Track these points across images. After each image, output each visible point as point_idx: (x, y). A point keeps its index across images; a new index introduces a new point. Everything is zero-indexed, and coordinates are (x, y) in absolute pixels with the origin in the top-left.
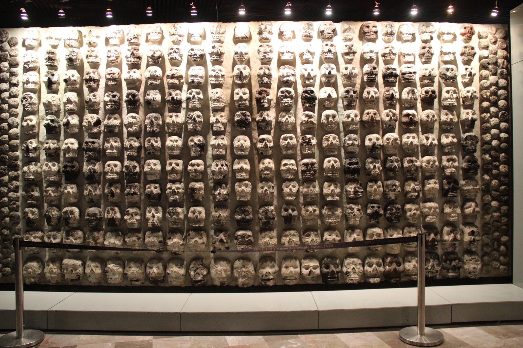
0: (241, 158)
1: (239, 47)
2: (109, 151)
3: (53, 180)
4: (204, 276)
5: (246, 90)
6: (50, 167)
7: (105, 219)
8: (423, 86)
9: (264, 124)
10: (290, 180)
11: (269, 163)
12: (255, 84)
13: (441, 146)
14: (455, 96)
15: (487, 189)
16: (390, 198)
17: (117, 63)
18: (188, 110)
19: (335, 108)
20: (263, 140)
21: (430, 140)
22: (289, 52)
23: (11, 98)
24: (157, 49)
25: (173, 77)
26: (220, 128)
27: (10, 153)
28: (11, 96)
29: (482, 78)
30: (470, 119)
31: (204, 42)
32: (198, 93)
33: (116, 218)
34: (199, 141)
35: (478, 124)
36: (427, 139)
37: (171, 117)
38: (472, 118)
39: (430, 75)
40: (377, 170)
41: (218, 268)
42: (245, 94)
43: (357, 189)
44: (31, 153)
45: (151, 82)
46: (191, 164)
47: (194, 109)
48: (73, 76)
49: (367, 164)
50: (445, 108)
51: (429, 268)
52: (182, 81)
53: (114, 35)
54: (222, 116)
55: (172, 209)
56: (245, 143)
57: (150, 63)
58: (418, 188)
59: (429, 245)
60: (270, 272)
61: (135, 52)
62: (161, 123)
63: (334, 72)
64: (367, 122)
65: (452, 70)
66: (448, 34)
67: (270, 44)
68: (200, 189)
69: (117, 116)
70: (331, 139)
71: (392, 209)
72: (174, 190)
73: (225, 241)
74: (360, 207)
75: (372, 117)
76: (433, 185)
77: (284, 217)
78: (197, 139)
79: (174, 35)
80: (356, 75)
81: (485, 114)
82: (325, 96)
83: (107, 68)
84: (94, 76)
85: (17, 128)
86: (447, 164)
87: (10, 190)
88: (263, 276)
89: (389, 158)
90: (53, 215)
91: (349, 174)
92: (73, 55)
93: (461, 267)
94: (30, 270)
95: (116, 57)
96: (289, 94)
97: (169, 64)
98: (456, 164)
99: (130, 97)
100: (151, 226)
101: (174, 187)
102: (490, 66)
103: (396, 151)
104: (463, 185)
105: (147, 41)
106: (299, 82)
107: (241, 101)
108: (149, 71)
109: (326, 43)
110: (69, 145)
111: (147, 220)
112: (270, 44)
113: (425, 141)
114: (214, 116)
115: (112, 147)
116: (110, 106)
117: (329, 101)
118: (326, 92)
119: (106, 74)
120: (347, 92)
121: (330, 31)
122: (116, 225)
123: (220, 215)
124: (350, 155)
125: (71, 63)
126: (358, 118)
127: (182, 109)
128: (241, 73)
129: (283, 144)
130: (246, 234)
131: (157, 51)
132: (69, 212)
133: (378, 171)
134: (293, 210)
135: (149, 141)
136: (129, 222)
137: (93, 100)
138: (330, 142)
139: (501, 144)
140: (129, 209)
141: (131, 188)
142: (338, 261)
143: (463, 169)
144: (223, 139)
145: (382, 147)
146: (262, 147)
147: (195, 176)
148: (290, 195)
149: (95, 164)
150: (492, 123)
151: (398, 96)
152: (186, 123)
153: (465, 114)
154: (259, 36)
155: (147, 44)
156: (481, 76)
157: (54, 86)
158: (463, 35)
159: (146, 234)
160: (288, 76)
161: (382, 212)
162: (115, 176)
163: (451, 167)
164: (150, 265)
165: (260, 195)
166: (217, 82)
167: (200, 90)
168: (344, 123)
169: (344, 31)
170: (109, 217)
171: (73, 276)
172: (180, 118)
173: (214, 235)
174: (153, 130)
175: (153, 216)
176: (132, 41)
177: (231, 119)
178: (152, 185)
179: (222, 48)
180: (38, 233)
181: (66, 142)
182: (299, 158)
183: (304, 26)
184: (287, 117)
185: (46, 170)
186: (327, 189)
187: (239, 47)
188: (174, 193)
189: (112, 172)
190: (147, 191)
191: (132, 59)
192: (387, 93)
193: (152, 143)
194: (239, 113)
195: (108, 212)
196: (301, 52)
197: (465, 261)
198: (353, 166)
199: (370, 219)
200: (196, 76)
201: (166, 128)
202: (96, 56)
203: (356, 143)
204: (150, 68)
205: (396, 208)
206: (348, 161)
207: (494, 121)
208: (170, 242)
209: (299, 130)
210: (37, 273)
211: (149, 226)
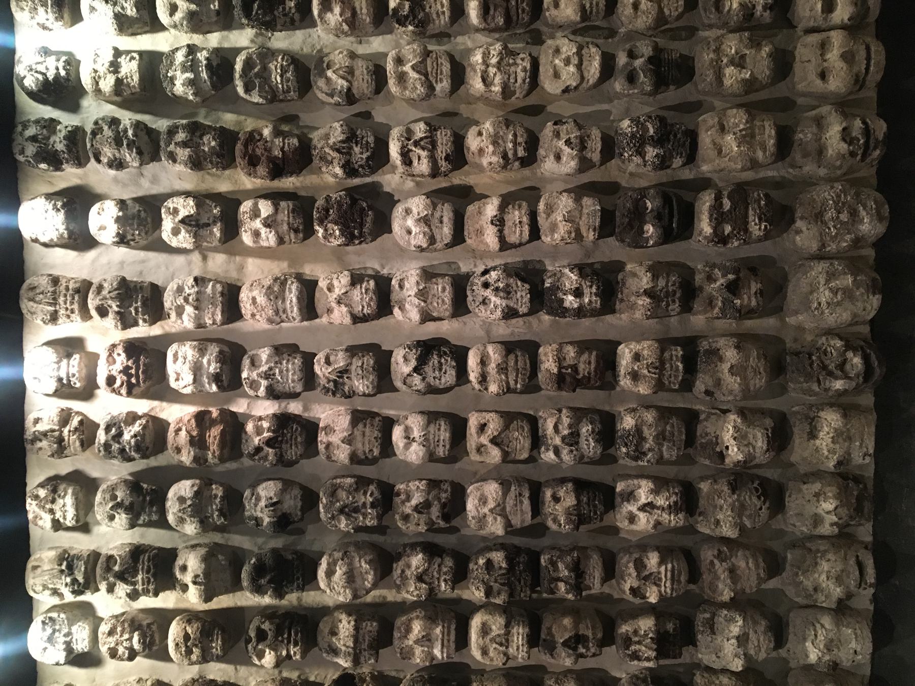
1: (102, 228)
2: (437, 652)
4: (848, 346)
17: (154, 627)
24: (108, 496)
25: (198, 442)
26: (367, 290)
33: (657, 632)
42: (255, 213)
46: (480, 383)
52: (215, 413)
53: (60, 639)
54: (330, 288)
55: (626, 445)
56: (415, 210)
57: (155, 517)
60: (841, 129)
62: (349, 481)
67: (89, 128)
72: (563, 439)
73: (731, 277)
83: (170, 660)
95: (132, 632)
97: (160, 456)
99: (263, 581)
105: (83, 527)
108: (181, 521)
112: (89, 128)
114: (329, 311)
115: (426, 640)
119: (186, 662)
123: (647, 293)
127: (306, 415)
135: (406, 518)
136: (667, 587)
159: (707, 531)
167: (246, 357)
170: (653, 654)
174: (373, 505)
175: (648, 507)
176: (81, 579)
179: (106, 285)
187: (102, 228)
188: (573, 439)
200: (197, 369)
208: (735, 454)
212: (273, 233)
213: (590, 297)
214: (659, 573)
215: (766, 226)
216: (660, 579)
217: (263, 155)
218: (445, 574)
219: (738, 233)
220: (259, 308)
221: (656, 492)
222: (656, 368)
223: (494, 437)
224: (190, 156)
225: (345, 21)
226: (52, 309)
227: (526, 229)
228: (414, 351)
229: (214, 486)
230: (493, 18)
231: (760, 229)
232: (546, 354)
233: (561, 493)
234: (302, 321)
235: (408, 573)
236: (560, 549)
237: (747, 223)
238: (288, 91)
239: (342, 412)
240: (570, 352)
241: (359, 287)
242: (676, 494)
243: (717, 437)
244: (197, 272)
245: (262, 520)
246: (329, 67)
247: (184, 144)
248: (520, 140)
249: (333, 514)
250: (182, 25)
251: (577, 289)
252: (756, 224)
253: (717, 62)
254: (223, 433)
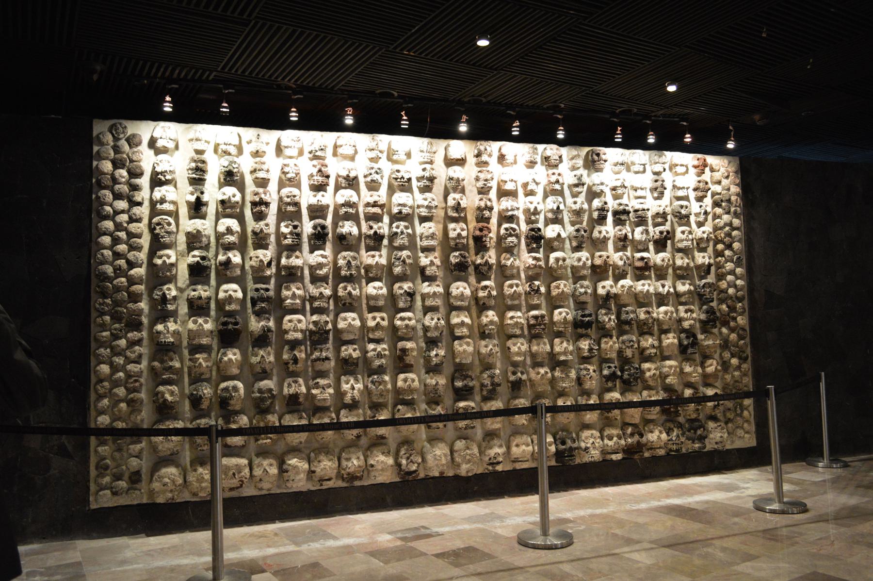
0: (459, 309)
1: (455, 172)
2: (288, 301)
3: (205, 343)
4: (419, 464)
5: (465, 226)
6: (201, 325)
7: (284, 396)
8: (655, 225)
9: (486, 268)
10: (516, 336)
12: (471, 217)
13: (678, 295)
14: (690, 236)
15: (725, 344)
16: (627, 356)
18: (392, 248)
19: (563, 250)
20: (486, 287)
21: (666, 288)
22: (512, 180)
23: (131, 223)
27: (130, 305)
28: (132, 220)
29: (715, 217)
30: (707, 263)
31: (408, 161)
32: (406, 228)
34: (409, 288)
35: (713, 269)
36: (663, 286)
37: (373, 256)
38: (709, 263)
39: (664, 213)
40: (612, 323)
41: (436, 452)
42: (463, 230)
44: (170, 304)
45: (346, 210)
47: (401, 248)
48: (234, 196)
49: (600, 317)
50: (680, 250)
51: (674, 439)
54: (435, 258)
58: (656, 343)
59: (673, 412)
61: (323, 169)
62: (359, 263)
63: (562, 207)
64: (599, 266)
65: (687, 207)
66: (682, 165)
68: (412, 349)
69: (297, 253)
70: (562, 286)
71: (630, 369)
72: (379, 352)
74: (595, 368)
75: (605, 260)
76: (670, 340)
77: (512, 382)
78: (407, 286)
79: (373, 150)
80: (585, 211)
81: (720, 258)
82: (554, 235)
84: (266, 198)
85: (141, 267)
86: (686, 316)
87: (129, 361)
88: (490, 459)
89: (624, 309)
90: (204, 395)
91: (581, 328)
92: (235, 166)
93: (706, 437)
94: (167, 480)
96: (514, 231)
97: (365, 187)
98: (694, 315)
99: (319, 228)
100: (351, 402)
101: (380, 348)
102: (723, 204)
103: (632, 301)
104: (702, 340)
105: (335, 154)
106: (522, 218)
107: (459, 239)
109: (551, 172)
110: (231, 293)
111: (344, 393)
113: (661, 289)
114: (426, 257)
115: (294, 296)
116: (290, 240)
117: (558, 241)
120: (578, 231)
121: (557, 158)
122: (300, 404)
123: (437, 383)
124: (580, 305)
125: (230, 177)
126: (589, 262)
128: (459, 204)
130: (470, 406)
131: (352, 169)
132: (231, 388)
134: (522, 373)
135: (345, 288)
137: (265, 231)
138: (560, 290)
139: (738, 292)
140: (318, 380)
141: (321, 351)
142: (574, 435)
143: (701, 321)
144: (438, 286)
145: (616, 296)
146: (485, 297)
147: (406, 334)
148: (518, 354)
149: (269, 320)
150: (727, 268)
151: (631, 237)
152: (390, 266)
153: (701, 258)
154: (475, 159)
155: (335, 159)
156: (715, 214)
157: (204, 209)
158: (695, 167)
160: (512, 210)
161: (619, 373)
162: (299, 336)
163: (689, 319)
164: (347, 456)
165: (481, 356)
166: (430, 214)
168: (573, 267)
169: (572, 159)
170: (291, 392)
171: (235, 482)
172: (380, 258)
173: (428, 409)
174: (351, 274)
175: (353, 388)
177: (445, 260)
178: (350, 346)
180: (178, 423)
181: (226, 289)
182: (524, 309)
183: (528, 150)
184: (512, 259)
185: (195, 329)
187: (455, 172)
188: (380, 356)
189: (295, 330)
190: (343, 354)
191: (320, 179)
192: (620, 233)
193: (350, 291)
194: (457, 254)
195: (289, 385)
196: (525, 181)
197: (710, 429)
198: (587, 319)
199: (607, 381)
200: (404, 205)
201: (363, 271)
202: (268, 171)
203: (589, 291)
204: (342, 192)
205: (634, 368)
206: (580, 313)
207: (729, 266)
209: (523, 275)
210: (178, 483)
211: (346, 402)
213: (435, 360)
226: (425, 151)
227: (460, 334)
233: (357, 352)
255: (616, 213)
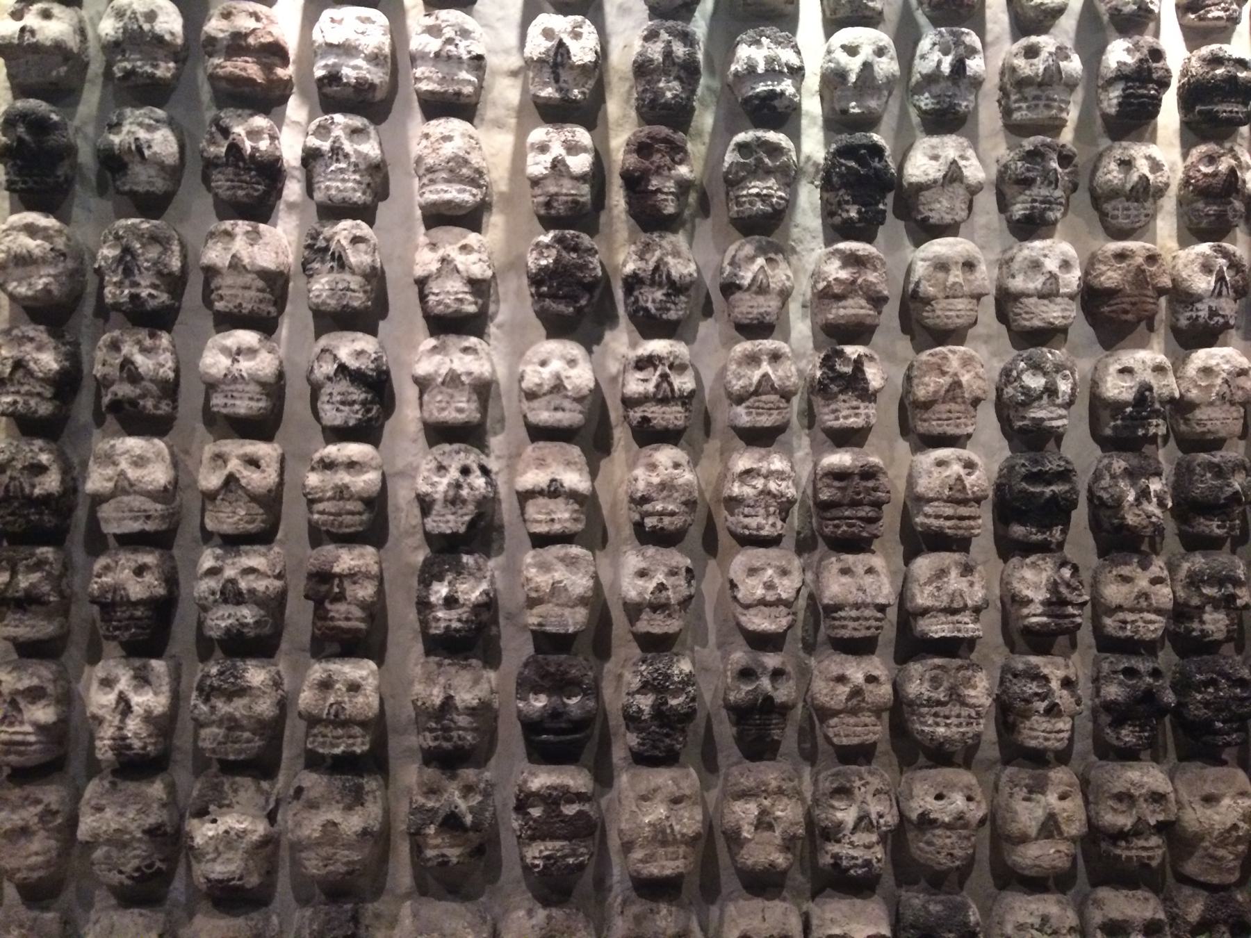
11: (677, 465)
25: (237, 45)
26: (461, 301)
40: (1152, 508)
42: (572, 148)
43: (1063, 590)
45: (129, 66)
46: (322, 460)
52: (281, 72)
54: (465, 248)
55: (221, 673)
56: (573, 372)
62: (175, 264)
72: (232, 581)
73: (469, 819)
80: (1071, 86)
114: (433, 246)
118: (935, 158)
123: (448, 701)
127: (281, 206)
129: (741, 383)
133: (1158, 512)
135: (115, 346)
138: (945, 381)
161: (1170, 698)
167: (366, 121)
174: (134, 297)
175: (124, 706)
186: (929, 589)
188: (232, 595)
192: (1209, 170)
198: (1048, 491)
200: (346, 49)
208: (203, 832)
212: (545, 172)
214: (22, 723)
215: (537, 866)
216: (11, 724)
217: (652, 163)
218: (26, 403)
219: (530, 828)
220: (436, 145)
221: (148, 718)
222: (336, 715)
223: (237, 480)
224: (651, 61)
225: (829, 286)
227: (542, 529)
228: (372, 366)
229: (172, 65)
230: (828, 486)
231: (535, 858)
232: (362, 556)
233: (148, 578)
234: (422, 207)
235: (28, 347)
236: (61, 576)
237: (543, 838)
238: (739, 204)
239: (282, 258)
240: (366, 591)
241: (466, 289)
242: (144, 748)
243: (229, 806)
244: (492, 61)
245: (118, 133)
246: (769, 260)
247: (668, 54)
248: (667, 520)
249: (122, 237)
250: (830, 61)
251: (456, 601)
252: (541, 852)
253: (764, 791)
254: (250, 81)
255: (1193, 95)
